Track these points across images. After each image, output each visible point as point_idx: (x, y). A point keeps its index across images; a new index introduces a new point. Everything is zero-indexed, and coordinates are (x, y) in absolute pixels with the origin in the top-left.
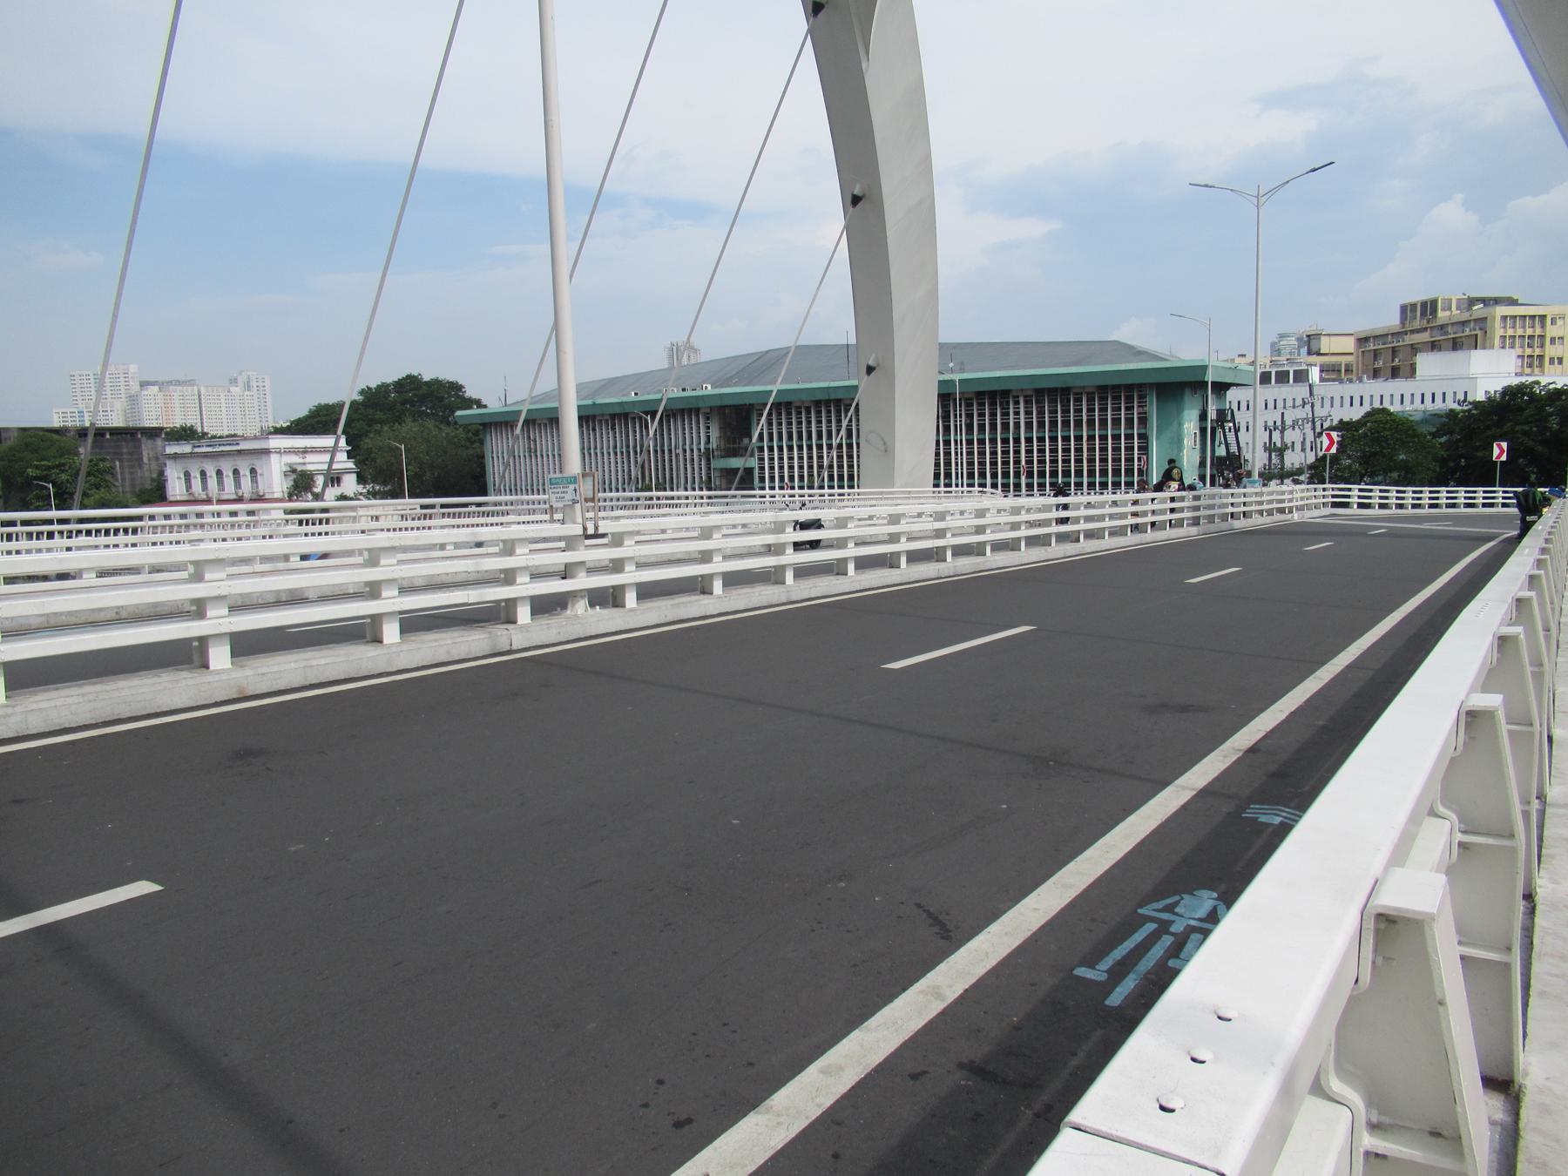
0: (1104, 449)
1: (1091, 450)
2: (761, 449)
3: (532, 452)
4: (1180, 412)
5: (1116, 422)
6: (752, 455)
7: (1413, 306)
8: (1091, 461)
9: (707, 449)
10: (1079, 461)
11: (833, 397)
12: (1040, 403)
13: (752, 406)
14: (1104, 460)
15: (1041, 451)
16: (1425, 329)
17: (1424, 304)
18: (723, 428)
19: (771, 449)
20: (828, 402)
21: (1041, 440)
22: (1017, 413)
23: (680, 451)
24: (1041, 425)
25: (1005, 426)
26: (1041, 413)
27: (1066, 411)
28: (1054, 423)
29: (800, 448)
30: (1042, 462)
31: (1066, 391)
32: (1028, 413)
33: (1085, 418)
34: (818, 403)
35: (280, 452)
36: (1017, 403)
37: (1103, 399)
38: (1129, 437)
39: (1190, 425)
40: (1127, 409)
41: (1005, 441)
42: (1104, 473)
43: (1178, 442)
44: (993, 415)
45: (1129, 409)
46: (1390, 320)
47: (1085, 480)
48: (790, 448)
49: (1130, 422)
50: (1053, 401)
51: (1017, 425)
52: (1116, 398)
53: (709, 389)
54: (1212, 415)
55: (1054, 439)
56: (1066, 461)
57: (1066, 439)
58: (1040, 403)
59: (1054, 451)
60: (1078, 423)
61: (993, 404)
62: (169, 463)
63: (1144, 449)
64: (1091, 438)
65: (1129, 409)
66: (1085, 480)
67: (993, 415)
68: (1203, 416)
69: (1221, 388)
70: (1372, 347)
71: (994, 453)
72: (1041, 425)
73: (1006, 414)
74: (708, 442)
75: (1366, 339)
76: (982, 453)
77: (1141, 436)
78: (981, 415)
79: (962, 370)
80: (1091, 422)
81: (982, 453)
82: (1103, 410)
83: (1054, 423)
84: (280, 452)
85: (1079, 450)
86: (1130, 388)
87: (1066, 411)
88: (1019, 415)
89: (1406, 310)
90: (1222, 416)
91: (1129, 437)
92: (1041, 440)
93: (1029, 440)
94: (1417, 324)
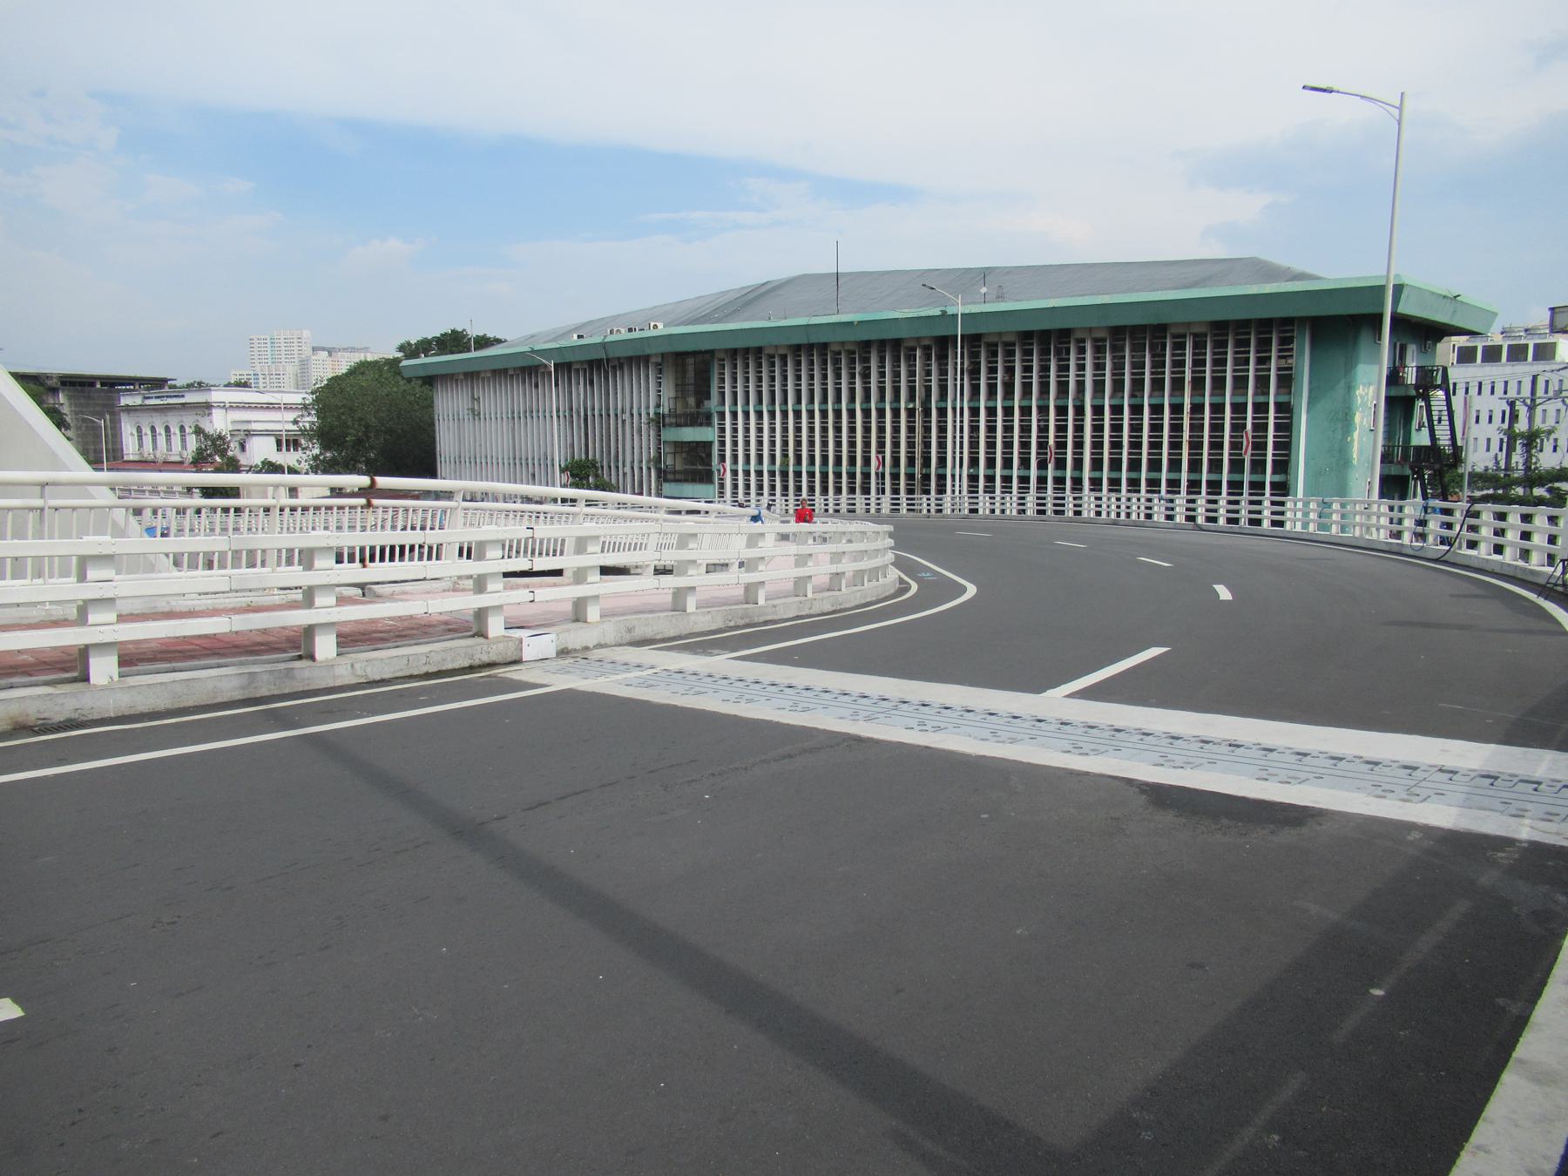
0: (1217, 428)
1: (1197, 428)
2: (722, 415)
3: (475, 414)
4: (1349, 367)
5: (1240, 383)
6: (709, 424)
8: (1196, 445)
9: (657, 414)
11: (814, 340)
12: (1117, 350)
13: (711, 352)
14: (1216, 446)
18: (681, 387)
19: (734, 415)
20: (810, 347)
21: (1117, 410)
22: (1081, 367)
23: (627, 416)
24: (1118, 386)
25: (1063, 387)
26: (1118, 367)
27: (1158, 364)
28: (1138, 384)
29: (772, 414)
30: (1116, 445)
31: (1160, 330)
32: (1099, 367)
33: (1188, 376)
35: (224, 407)
36: (1082, 350)
37: (1221, 345)
38: (1261, 408)
39: (1368, 389)
40: (1260, 361)
41: (1062, 411)
43: (1345, 419)
44: (1045, 369)
45: (1263, 361)
47: (1184, 476)
48: (759, 414)
49: (1263, 383)
50: (1138, 349)
51: (1081, 385)
52: (1243, 344)
53: (662, 329)
54: (1411, 377)
55: (1137, 410)
56: (1156, 445)
57: (1157, 409)
58: (1117, 350)
59: (1136, 428)
60: (1178, 384)
61: (1045, 352)
62: (124, 418)
63: (1286, 427)
64: (1197, 409)
65: (1263, 361)
68: (1394, 378)
69: (1427, 332)
72: (1118, 386)
74: (658, 406)
76: (1026, 429)
77: (1280, 407)
79: (1000, 298)
80: (1198, 383)
81: (1026, 429)
82: (1220, 362)
83: (1138, 384)
84: (224, 407)
85: (1176, 428)
86: (1265, 325)
87: (1158, 364)
88: (1083, 369)
90: (1425, 374)
91: (1261, 408)
92: (1117, 410)
93: (1098, 410)
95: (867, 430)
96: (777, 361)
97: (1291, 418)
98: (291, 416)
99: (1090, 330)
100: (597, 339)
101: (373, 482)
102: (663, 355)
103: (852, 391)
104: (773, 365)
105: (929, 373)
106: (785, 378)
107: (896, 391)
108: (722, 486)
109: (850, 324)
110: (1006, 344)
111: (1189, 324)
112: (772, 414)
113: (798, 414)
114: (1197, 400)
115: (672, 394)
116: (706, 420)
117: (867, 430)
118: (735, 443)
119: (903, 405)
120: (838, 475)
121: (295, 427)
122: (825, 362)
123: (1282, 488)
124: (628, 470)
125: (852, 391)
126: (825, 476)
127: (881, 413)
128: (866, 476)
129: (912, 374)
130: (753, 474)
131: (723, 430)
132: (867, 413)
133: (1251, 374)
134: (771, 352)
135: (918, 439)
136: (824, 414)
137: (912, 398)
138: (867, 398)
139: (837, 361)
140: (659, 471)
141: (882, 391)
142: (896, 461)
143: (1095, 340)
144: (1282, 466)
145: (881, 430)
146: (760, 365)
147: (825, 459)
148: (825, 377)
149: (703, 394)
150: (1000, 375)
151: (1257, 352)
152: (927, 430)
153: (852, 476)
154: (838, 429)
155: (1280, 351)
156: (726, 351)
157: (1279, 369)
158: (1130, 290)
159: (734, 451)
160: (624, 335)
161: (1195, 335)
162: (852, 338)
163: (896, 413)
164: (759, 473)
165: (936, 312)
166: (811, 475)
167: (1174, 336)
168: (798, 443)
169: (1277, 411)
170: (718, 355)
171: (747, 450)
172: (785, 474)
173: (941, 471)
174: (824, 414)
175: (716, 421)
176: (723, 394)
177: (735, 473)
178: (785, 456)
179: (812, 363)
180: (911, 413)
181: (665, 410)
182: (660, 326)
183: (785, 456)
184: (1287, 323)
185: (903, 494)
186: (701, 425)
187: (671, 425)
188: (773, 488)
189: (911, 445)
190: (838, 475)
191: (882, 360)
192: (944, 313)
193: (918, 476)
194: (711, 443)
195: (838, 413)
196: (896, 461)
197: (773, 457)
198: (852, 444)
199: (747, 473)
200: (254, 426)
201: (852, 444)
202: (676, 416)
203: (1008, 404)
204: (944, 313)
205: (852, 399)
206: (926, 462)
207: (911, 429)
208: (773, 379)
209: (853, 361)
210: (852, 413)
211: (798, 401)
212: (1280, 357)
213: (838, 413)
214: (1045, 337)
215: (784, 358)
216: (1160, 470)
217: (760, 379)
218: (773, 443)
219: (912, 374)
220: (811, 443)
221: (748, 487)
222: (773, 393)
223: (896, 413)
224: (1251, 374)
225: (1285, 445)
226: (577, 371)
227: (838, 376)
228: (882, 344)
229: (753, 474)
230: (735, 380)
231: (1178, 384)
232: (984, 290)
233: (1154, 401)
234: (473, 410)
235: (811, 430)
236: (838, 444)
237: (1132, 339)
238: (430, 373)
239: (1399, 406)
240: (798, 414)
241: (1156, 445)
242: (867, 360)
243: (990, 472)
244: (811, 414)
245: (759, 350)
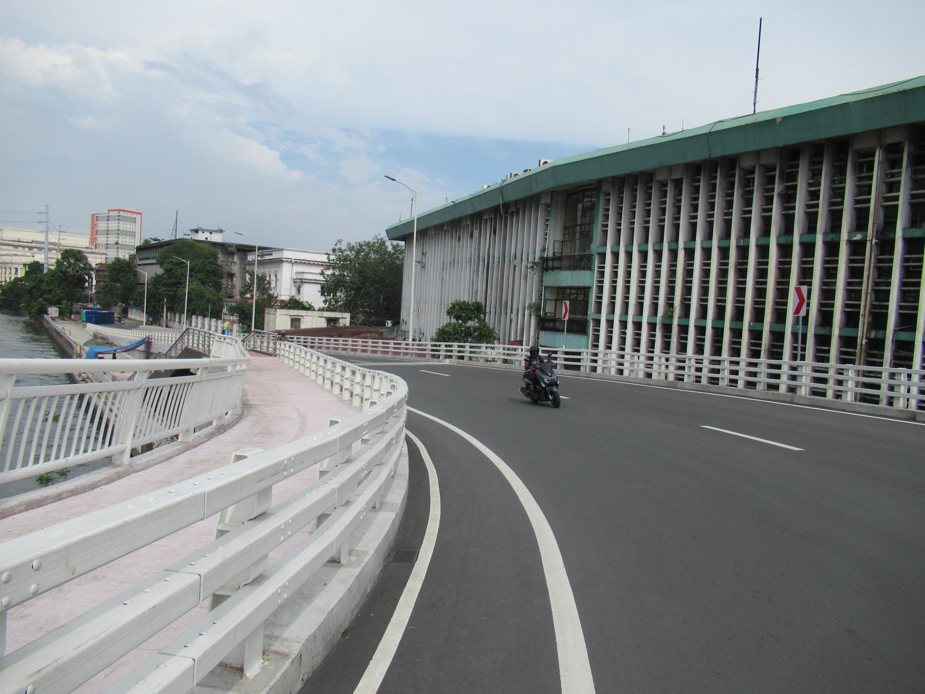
2: (603, 256)
6: (589, 268)
9: (542, 258)
11: (717, 153)
18: (568, 230)
19: (616, 255)
29: (658, 254)
96: (670, 190)
98: (318, 270)
102: (553, 193)
103: (766, 222)
105: (893, 187)
108: (597, 338)
112: (658, 254)
113: (690, 253)
115: (559, 237)
116: (582, 262)
119: (844, 236)
120: (737, 333)
122: (731, 186)
124: (514, 316)
125: (766, 222)
126: (718, 333)
127: (808, 249)
128: (778, 336)
129: (863, 190)
130: (630, 326)
131: (602, 274)
132: (785, 250)
135: (867, 286)
136: (724, 252)
137: (860, 223)
138: (788, 229)
139: (748, 183)
140: (538, 316)
141: (811, 219)
142: (826, 318)
147: (720, 311)
149: (587, 237)
153: (756, 335)
154: (742, 273)
163: (832, 249)
164: (638, 325)
166: (701, 330)
168: (687, 290)
172: (667, 328)
174: (724, 252)
175: (596, 263)
177: (610, 323)
178: (670, 304)
180: (857, 248)
183: (670, 304)
185: (833, 363)
187: (553, 268)
188: (652, 344)
189: (853, 294)
190: (737, 333)
191: (816, 175)
193: (862, 341)
194: (589, 288)
195: (743, 251)
196: (826, 318)
197: (655, 306)
199: (624, 324)
200: (306, 276)
201: (760, 293)
205: (765, 231)
206: (879, 320)
207: (855, 272)
208: (663, 211)
215: (678, 184)
217: (648, 213)
218: (656, 290)
219: (863, 190)
220: (705, 291)
221: (623, 340)
223: (832, 249)
226: (486, 220)
227: (748, 202)
229: (630, 326)
235: (706, 273)
236: (740, 292)
242: (793, 177)
244: (707, 252)
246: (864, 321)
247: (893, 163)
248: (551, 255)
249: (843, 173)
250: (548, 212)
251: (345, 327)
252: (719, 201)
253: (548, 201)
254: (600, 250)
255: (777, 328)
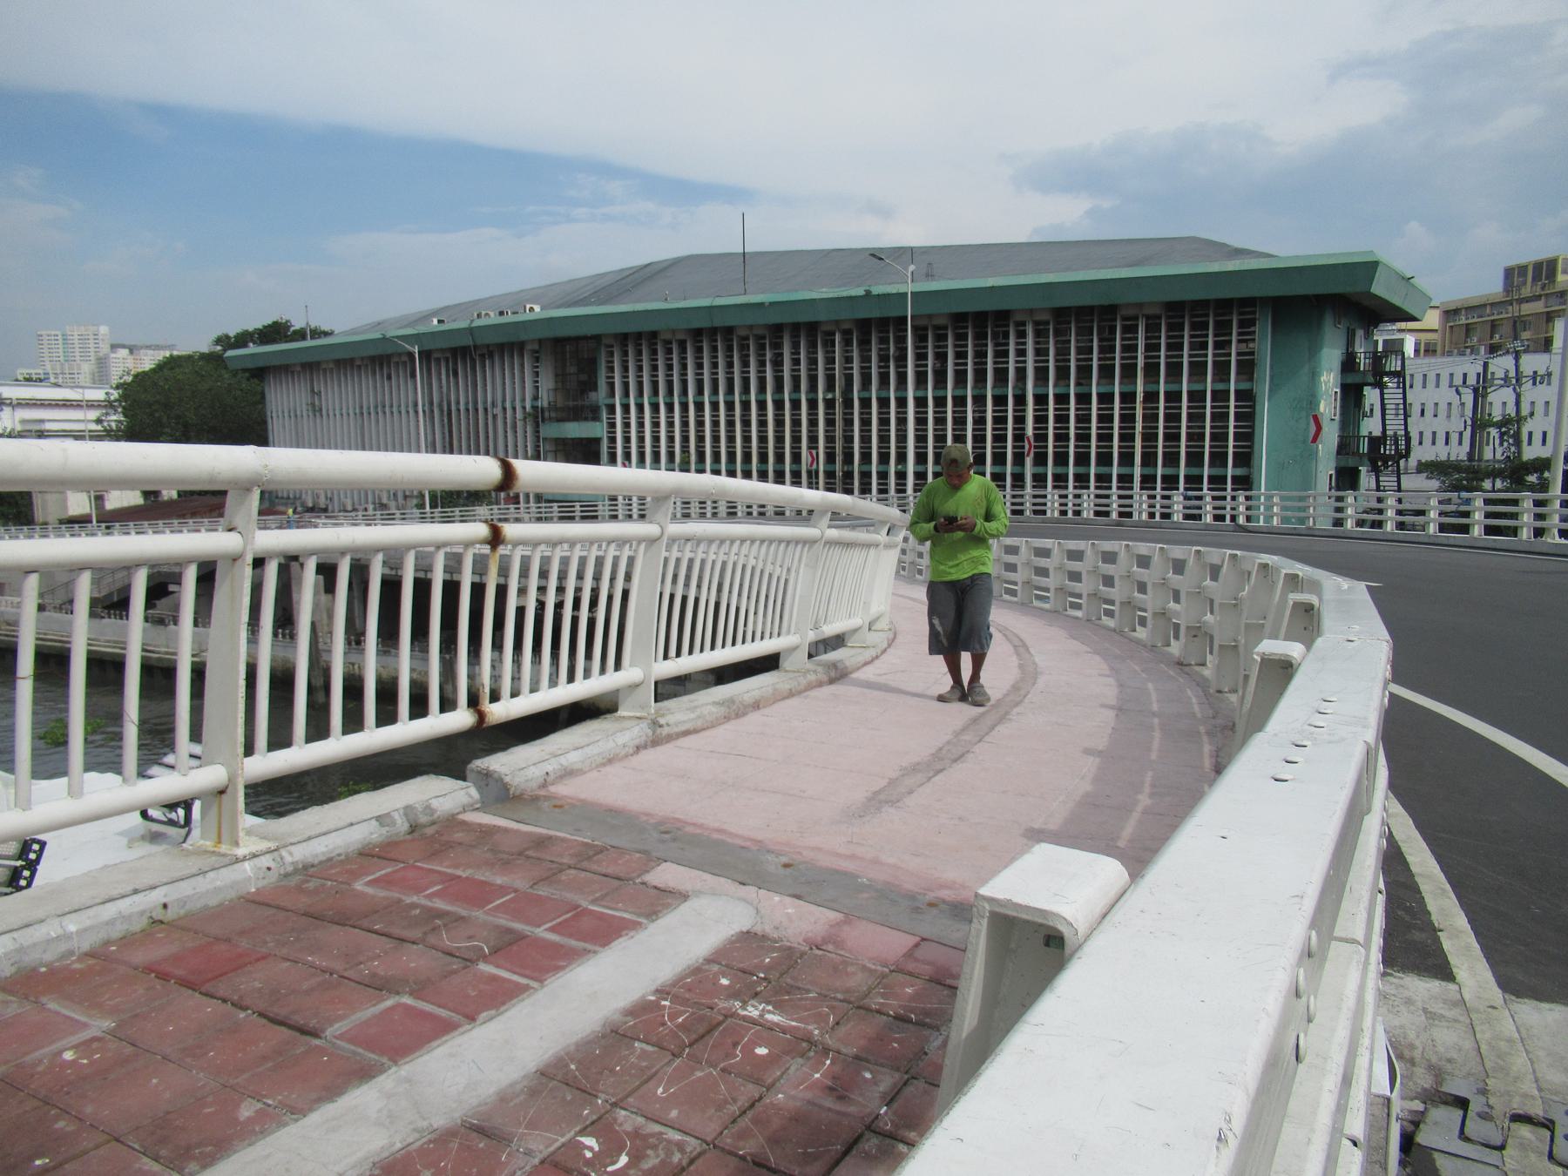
0: (1173, 418)
2: (612, 409)
3: (316, 410)
4: (1314, 351)
5: (1198, 369)
6: (596, 418)
7: (1522, 269)
8: (1149, 437)
9: (534, 408)
10: (1127, 438)
11: (718, 323)
12: (1061, 333)
13: (597, 338)
14: (1172, 437)
15: (1062, 419)
16: (1538, 298)
17: (1538, 266)
18: (561, 377)
19: (626, 408)
20: (713, 332)
21: (1062, 399)
22: (1021, 353)
23: (498, 410)
24: (1063, 373)
25: (1001, 376)
26: (1062, 353)
27: (1108, 349)
28: (1084, 372)
31: (1109, 312)
32: (1041, 352)
33: (1140, 362)
34: (697, 334)
36: (1022, 334)
37: (1176, 328)
40: (1217, 345)
41: (1000, 400)
42: (1171, 459)
44: (981, 355)
46: (1491, 286)
47: (1137, 471)
48: (655, 408)
49: (1222, 370)
50: (1084, 332)
51: (1021, 373)
55: (1083, 399)
56: (1105, 438)
58: (1061, 333)
59: (1083, 419)
61: (980, 337)
63: (1247, 417)
64: (1151, 397)
66: (1137, 471)
67: (981, 355)
68: (1349, 364)
70: (1463, 321)
71: (980, 421)
72: (1063, 373)
73: (1002, 354)
74: (536, 398)
75: (1456, 312)
77: (1240, 395)
78: (961, 355)
79: (929, 276)
80: (1151, 370)
82: (1176, 347)
83: (1084, 372)
85: (1128, 419)
86: (1224, 306)
87: (1108, 349)
89: (1513, 275)
92: (1062, 399)
93: (1041, 400)
94: (1527, 291)
95: (779, 423)
97: (1253, 407)
98: (93, 414)
99: (1031, 311)
100: (463, 324)
101: (509, 474)
102: (540, 341)
104: (669, 351)
105: (849, 360)
106: (684, 367)
107: (813, 381)
109: (761, 305)
110: (937, 328)
111: (1140, 305)
114: (1152, 388)
115: (551, 385)
116: (593, 414)
117: (779, 423)
118: (627, 440)
121: (99, 427)
123: (1244, 483)
127: (796, 405)
129: (830, 361)
131: (612, 425)
132: (779, 405)
133: (1210, 359)
134: (668, 336)
135: (839, 433)
137: (830, 387)
138: (779, 387)
139: (744, 348)
141: (796, 381)
143: (1036, 323)
144: (1244, 459)
145: (796, 423)
146: (654, 352)
148: (730, 365)
150: (930, 362)
151: (1215, 335)
152: (849, 422)
154: (746, 423)
155: (1239, 334)
156: (616, 336)
157: (1239, 354)
158: (1067, 269)
159: (641, 446)
160: (494, 319)
161: (1148, 317)
162: (762, 322)
163: (813, 404)
165: (860, 292)
167: (1124, 319)
168: (700, 439)
169: (1190, 400)
170: (604, 341)
171: (641, 446)
173: (865, 468)
175: (604, 415)
176: (611, 386)
179: (715, 349)
180: (830, 404)
181: (544, 402)
182: (537, 308)
184: (1247, 303)
186: (586, 419)
192: (868, 293)
193: (839, 474)
194: (598, 441)
195: (746, 405)
198: (763, 439)
200: (48, 426)
201: (763, 439)
202: (556, 409)
203: (940, 393)
204: (868, 293)
206: (848, 458)
207: (830, 422)
208: (670, 367)
209: (762, 347)
210: (762, 405)
211: (700, 391)
212: (1239, 341)
213: (746, 405)
214: (980, 318)
215: (682, 346)
216: (1111, 465)
218: (671, 439)
219: (830, 361)
220: (716, 439)
222: (670, 384)
223: (813, 404)
224: (1210, 359)
225: (1247, 437)
226: (438, 360)
228: (796, 328)
230: (626, 369)
231: (1129, 372)
232: (912, 268)
233: (1103, 390)
234: (313, 405)
235: (716, 424)
236: (747, 439)
237: (1077, 321)
238: (261, 364)
239: (1351, 395)
240: (699, 407)
241: (1105, 438)
243: (920, 468)
244: (715, 406)
245: (654, 335)
246: (839, 459)
247: (847, 342)
248: (545, 404)
249: (815, 346)
250: (537, 360)
251: (171, 502)
252: (721, 361)
253: (536, 347)
254: (609, 401)
255: (779, 467)
